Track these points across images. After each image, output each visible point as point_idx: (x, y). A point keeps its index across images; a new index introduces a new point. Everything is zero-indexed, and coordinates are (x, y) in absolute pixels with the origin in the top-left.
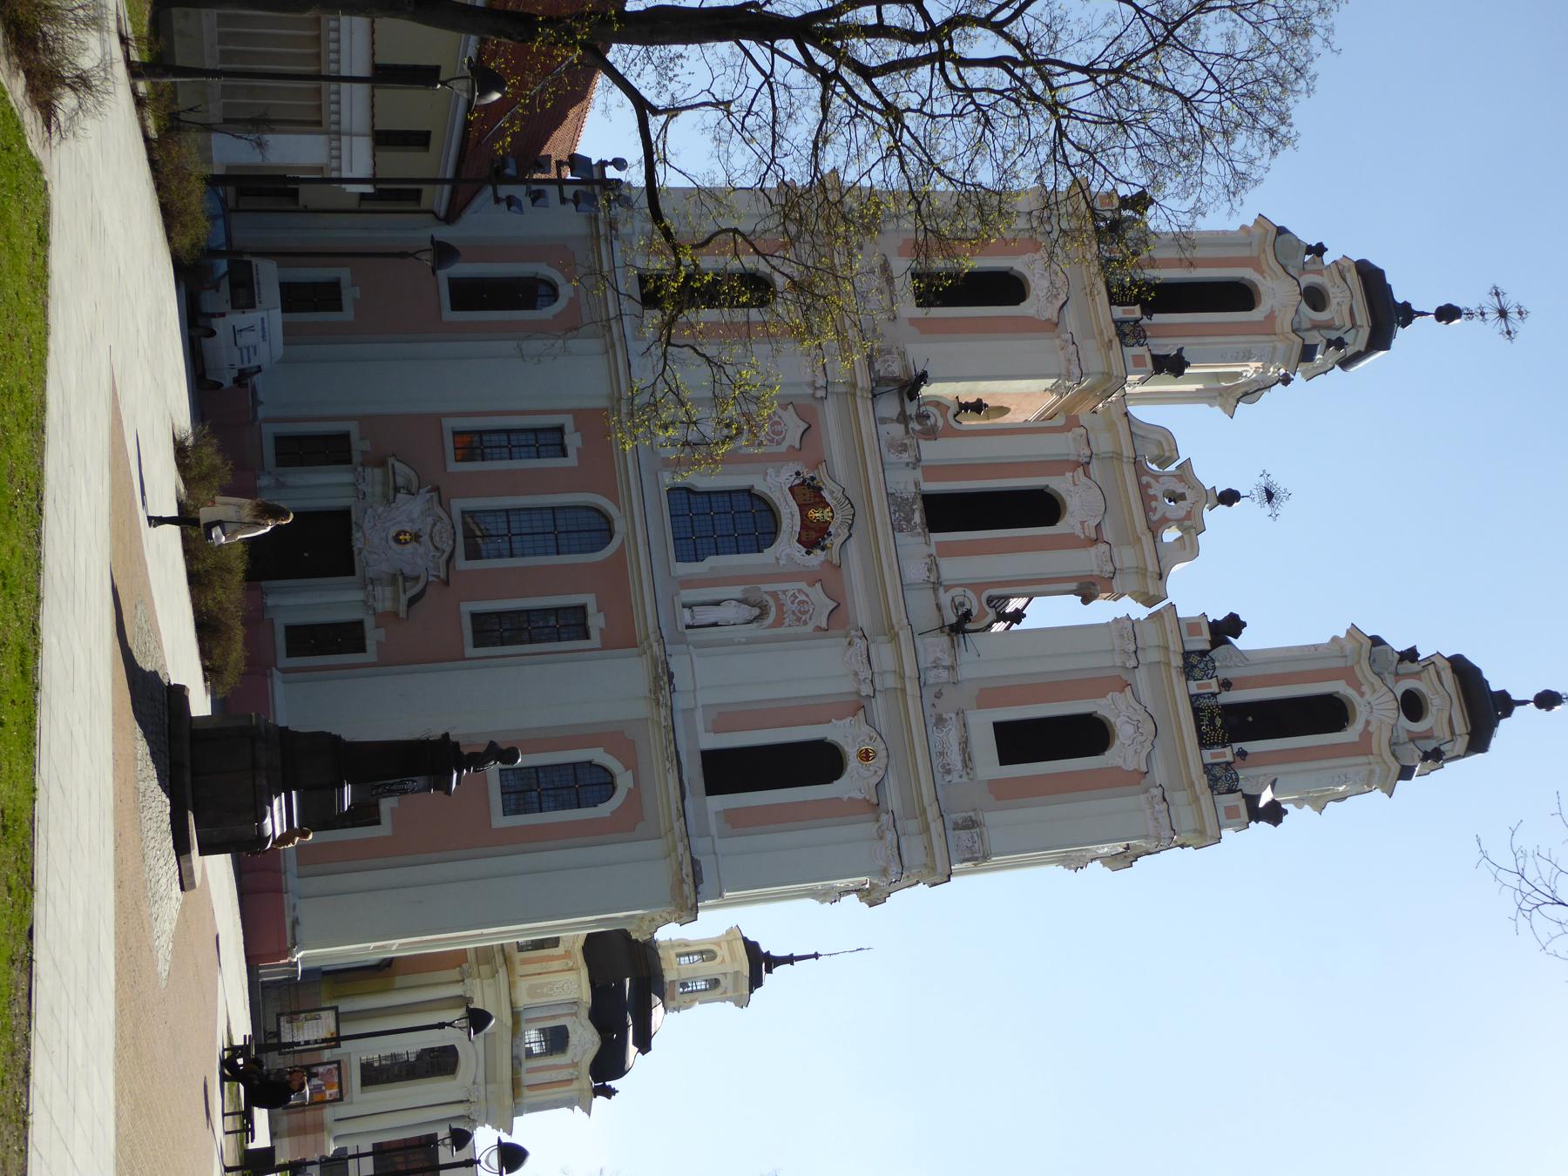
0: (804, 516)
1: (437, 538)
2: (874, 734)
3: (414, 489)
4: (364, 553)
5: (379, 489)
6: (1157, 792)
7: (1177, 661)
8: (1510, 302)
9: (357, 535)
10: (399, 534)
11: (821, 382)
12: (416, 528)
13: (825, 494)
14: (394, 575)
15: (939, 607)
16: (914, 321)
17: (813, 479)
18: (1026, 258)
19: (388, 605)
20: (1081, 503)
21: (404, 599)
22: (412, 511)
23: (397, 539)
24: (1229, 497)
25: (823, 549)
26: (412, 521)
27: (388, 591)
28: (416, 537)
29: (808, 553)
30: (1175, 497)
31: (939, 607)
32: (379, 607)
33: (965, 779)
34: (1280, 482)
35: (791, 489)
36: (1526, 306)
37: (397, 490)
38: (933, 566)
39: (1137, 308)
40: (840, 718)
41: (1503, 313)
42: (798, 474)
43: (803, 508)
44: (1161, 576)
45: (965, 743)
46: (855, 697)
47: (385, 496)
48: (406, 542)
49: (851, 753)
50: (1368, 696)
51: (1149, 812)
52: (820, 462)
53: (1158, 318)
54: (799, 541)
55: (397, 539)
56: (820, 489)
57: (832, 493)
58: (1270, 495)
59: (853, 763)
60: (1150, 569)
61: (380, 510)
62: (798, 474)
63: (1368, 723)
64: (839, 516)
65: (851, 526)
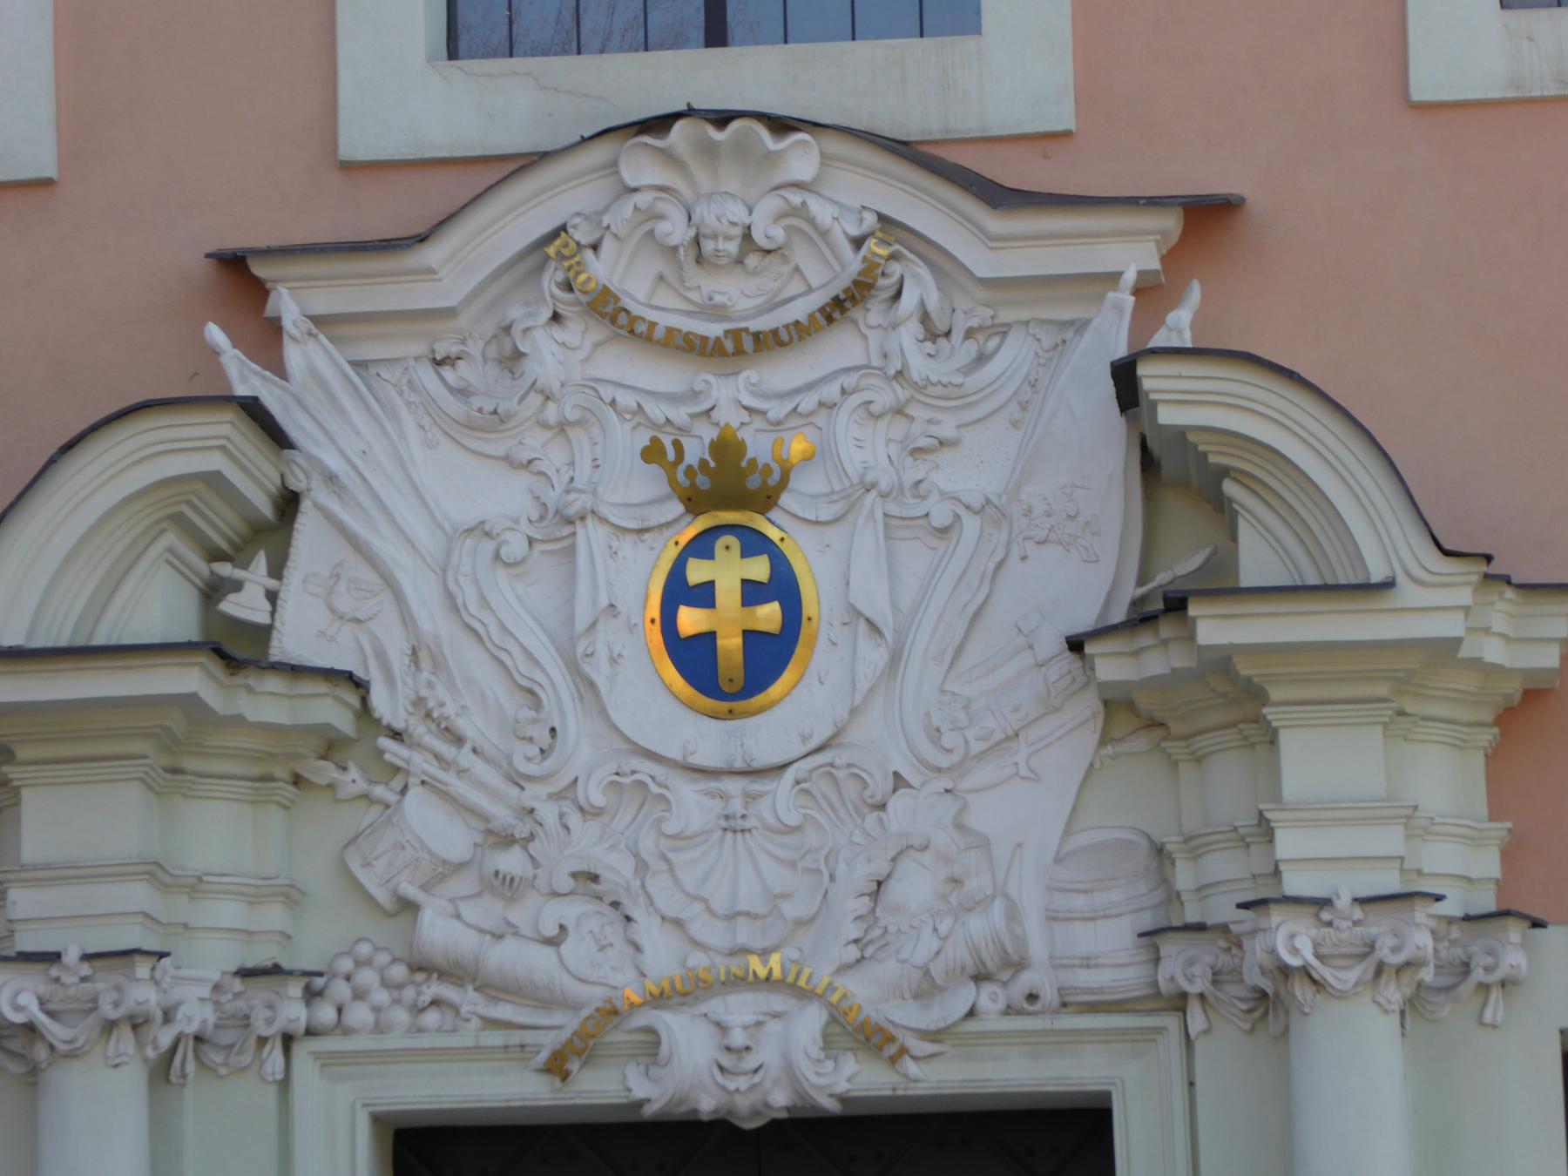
1: (742, 296)
3: (254, 478)
4: (865, 993)
5: (219, 832)
9: (691, 1068)
10: (695, 658)
12: (636, 489)
14: (1121, 710)
19: (1444, 775)
21: (1435, 604)
22: (462, 522)
23: (728, 675)
26: (562, 524)
27: (1321, 758)
28: (727, 491)
32: (1466, 865)
37: (236, 649)
47: (292, 771)
48: (781, 586)
55: (728, 675)
61: (430, 825)
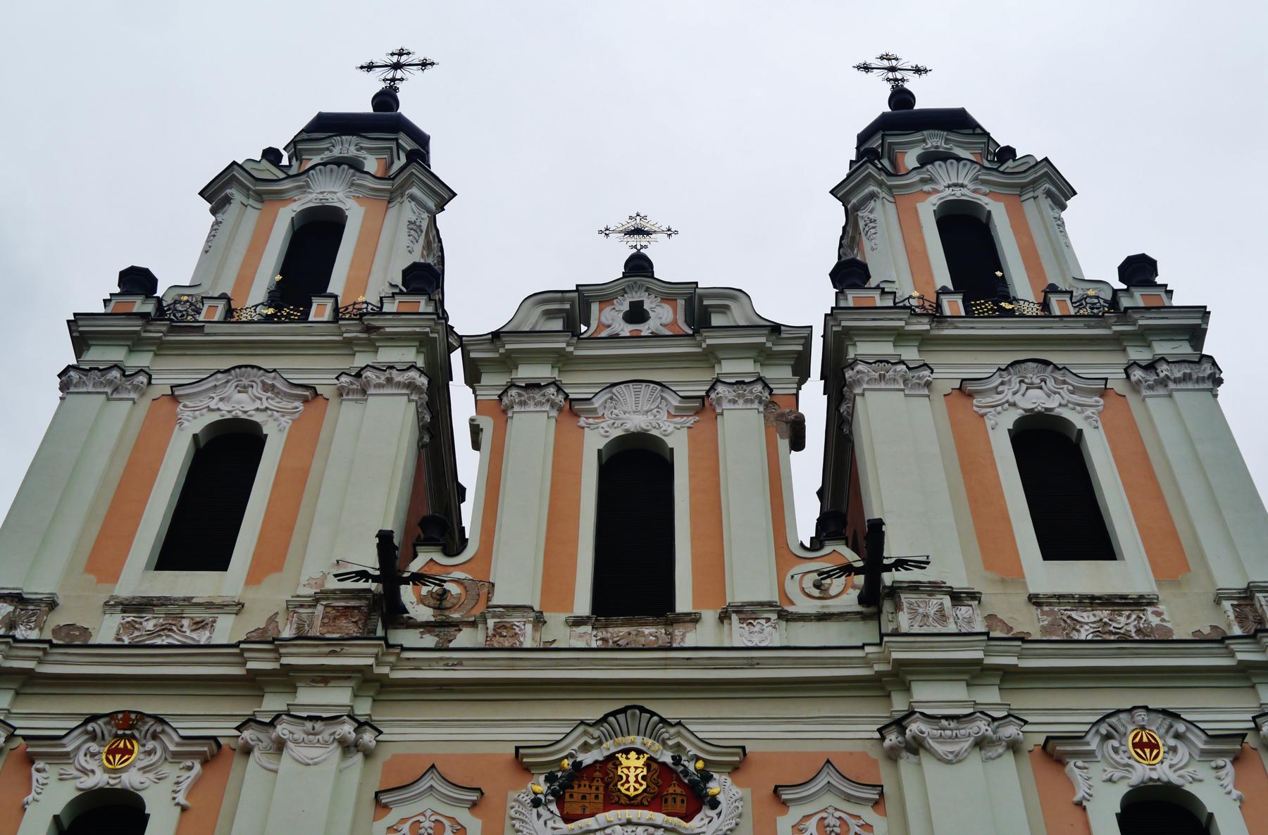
0: (632, 803)
2: (1104, 729)
6: (1137, 374)
7: (923, 325)
8: (382, 58)
11: (347, 729)
13: (587, 759)
15: (822, 617)
16: (254, 577)
17: (550, 779)
18: (187, 414)
20: (637, 413)
24: (639, 266)
25: (707, 777)
29: (714, 804)
30: (637, 314)
31: (822, 617)
33: (1161, 608)
34: (621, 219)
35: (568, 819)
36: (396, 49)
38: (748, 612)
39: (316, 302)
40: (1071, 785)
41: (397, 66)
42: (536, 803)
43: (613, 800)
44: (775, 329)
45: (1093, 601)
46: (1026, 761)
49: (1141, 772)
50: (940, 187)
51: (1172, 386)
52: (522, 763)
53: (336, 284)
54: (687, 818)
56: (577, 765)
57: (586, 747)
58: (638, 231)
59: (1164, 771)
60: (763, 340)
62: (536, 803)
63: (975, 191)
64: (637, 741)
65: (663, 720)
